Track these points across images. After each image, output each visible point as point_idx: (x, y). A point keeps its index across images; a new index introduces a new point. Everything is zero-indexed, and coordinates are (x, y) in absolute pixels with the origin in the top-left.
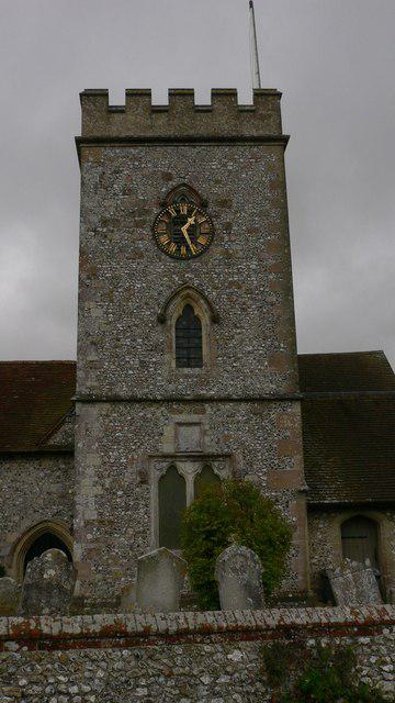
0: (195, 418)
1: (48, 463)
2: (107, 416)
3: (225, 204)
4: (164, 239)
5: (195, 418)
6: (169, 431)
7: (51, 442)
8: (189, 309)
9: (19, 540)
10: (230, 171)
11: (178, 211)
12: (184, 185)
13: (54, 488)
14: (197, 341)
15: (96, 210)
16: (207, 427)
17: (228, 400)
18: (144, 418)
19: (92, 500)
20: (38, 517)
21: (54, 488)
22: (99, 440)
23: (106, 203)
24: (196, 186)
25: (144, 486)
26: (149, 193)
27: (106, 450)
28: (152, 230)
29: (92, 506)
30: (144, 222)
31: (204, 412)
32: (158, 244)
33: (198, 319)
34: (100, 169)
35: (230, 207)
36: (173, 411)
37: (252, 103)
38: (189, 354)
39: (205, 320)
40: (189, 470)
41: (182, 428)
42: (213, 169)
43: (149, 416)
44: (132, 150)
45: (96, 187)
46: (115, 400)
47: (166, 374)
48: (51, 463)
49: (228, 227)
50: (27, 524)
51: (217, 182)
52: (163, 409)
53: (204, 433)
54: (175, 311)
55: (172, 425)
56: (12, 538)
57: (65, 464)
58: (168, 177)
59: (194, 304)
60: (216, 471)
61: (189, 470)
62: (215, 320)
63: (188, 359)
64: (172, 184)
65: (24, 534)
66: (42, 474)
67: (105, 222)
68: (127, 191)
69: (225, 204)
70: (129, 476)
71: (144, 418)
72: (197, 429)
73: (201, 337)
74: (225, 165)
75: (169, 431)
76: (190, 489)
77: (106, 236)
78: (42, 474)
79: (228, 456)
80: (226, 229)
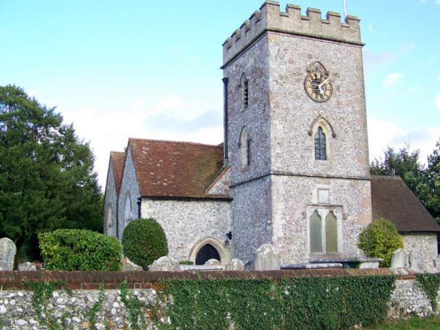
1: (208, 204)
4: (310, 90)
6: (315, 192)
7: (210, 192)
8: (320, 128)
9: (194, 247)
10: (338, 58)
11: (316, 76)
12: (319, 62)
13: (212, 219)
16: (331, 191)
17: (341, 178)
18: (303, 185)
19: (281, 227)
20: (203, 234)
21: (212, 219)
22: (283, 196)
25: (304, 220)
26: (302, 64)
27: (286, 200)
28: (304, 84)
29: (281, 230)
30: (300, 79)
31: (330, 183)
34: (278, 47)
35: (339, 77)
36: (316, 182)
38: (321, 153)
39: (328, 136)
40: (324, 212)
41: (321, 192)
42: (331, 54)
46: (291, 175)
47: (313, 165)
49: (338, 88)
50: (197, 238)
51: (333, 63)
53: (330, 194)
54: (315, 130)
56: (190, 246)
58: (310, 57)
59: (323, 127)
61: (324, 212)
62: (334, 136)
64: (313, 60)
65: (197, 244)
66: (206, 211)
67: (281, 77)
69: (336, 75)
70: (298, 215)
71: (303, 185)
72: (327, 192)
73: (325, 145)
74: (336, 55)
75: (315, 192)
78: (206, 211)
79: (341, 206)
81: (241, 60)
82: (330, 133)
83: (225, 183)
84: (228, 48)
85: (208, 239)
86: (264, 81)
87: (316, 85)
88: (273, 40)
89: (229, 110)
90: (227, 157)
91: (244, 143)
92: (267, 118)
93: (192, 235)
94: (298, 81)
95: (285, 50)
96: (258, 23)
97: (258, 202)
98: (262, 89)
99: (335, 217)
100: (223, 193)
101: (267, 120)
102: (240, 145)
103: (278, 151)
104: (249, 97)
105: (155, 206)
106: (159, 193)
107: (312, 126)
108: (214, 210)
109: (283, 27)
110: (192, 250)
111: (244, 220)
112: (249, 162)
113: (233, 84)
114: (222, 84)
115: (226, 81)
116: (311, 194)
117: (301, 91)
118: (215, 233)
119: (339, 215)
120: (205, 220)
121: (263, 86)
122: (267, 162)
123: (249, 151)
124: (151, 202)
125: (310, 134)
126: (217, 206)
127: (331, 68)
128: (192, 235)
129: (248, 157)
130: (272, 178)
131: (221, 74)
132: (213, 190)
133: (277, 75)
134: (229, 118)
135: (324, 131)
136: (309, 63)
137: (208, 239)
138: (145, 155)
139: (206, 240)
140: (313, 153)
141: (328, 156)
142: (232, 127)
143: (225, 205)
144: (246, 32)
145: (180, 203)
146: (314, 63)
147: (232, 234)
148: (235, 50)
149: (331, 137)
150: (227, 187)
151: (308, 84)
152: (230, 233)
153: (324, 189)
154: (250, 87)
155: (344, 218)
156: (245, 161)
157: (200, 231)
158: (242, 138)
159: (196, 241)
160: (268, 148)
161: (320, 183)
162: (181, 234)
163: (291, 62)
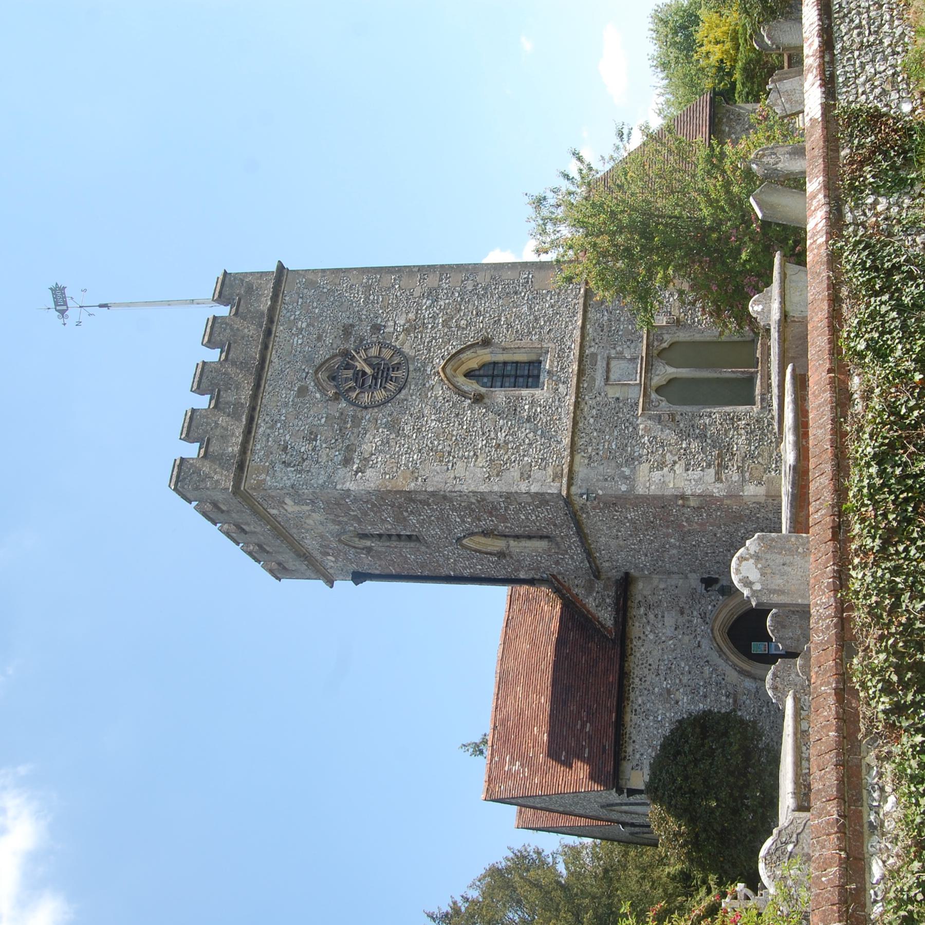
0: (601, 365)
1: (635, 629)
2: (590, 458)
3: (347, 331)
4: (380, 395)
5: (601, 365)
6: (613, 392)
7: (610, 623)
8: (469, 375)
9: (734, 666)
10: (308, 326)
11: (347, 380)
12: (316, 372)
14: (509, 368)
15: (330, 470)
16: (613, 352)
18: (596, 418)
20: (705, 643)
21: (670, 620)
22: (619, 466)
23: (323, 459)
24: (317, 362)
25: (678, 418)
28: (366, 408)
29: (696, 474)
31: (594, 355)
32: (384, 403)
33: (483, 366)
35: (352, 326)
37: (229, 307)
39: (485, 356)
40: (665, 372)
41: (613, 377)
43: (594, 412)
44: (261, 430)
45: (300, 472)
48: (637, 624)
49: (376, 328)
50: (714, 657)
51: (319, 338)
52: (587, 398)
53: (620, 356)
54: (471, 386)
55: (608, 388)
56: (732, 676)
57: (639, 607)
58: (303, 391)
59: (464, 368)
60: (665, 345)
61: (665, 372)
62: (486, 342)
63: (529, 376)
65: (727, 659)
66: (651, 637)
68: (312, 437)
69: (347, 331)
71: (596, 418)
72: (613, 363)
73: (505, 363)
74: (302, 329)
75: (613, 392)
76: (684, 372)
77: (365, 459)
78: (651, 637)
80: (380, 330)
81: (311, 544)
82: (481, 351)
83: (590, 589)
84: (285, 568)
85: (717, 633)
86: (355, 500)
87: (369, 381)
88: (263, 476)
89: (426, 573)
91: (497, 545)
92: (441, 498)
93: (707, 670)
95: (285, 449)
96: (224, 508)
97: (632, 521)
98: (374, 505)
99: (672, 345)
100: (612, 593)
101: (445, 497)
103: (515, 473)
104: (393, 532)
105: (638, 756)
106: (608, 744)
107: (463, 394)
108: (651, 616)
110: (742, 672)
111: (675, 551)
112: (542, 537)
113: (367, 563)
114: (368, 584)
115: (358, 577)
116: (618, 399)
117: (382, 416)
118: (703, 616)
120: (671, 638)
121: (367, 502)
122: (541, 499)
123: (517, 537)
124: (627, 766)
125: (478, 399)
126: (642, 610)
127: (331, 342)
128: (707, 670)
129: (530, 537)
130: (579, 491)
131: (344, 586)
132: (606, 616)
134: (444, 572)
135: (474, 364)
136: (318, 395)
137: (717, 633)
138: (522, 765)
139: (719, 639)
140: (525, 392)
141: (533, 357)
142: (465, 568)
143: (641, 589)
144: (245, 532)
145: (632, 696)
146: (318, 384)
147: (705, 576)
148: (288, 558)
149: (488, 350)
150: (599, 585)
151: (365, 398)
152: (703, 580)
153: (608, 370)
154: (369, 529)
156: (542, 545)
157: (698, 652)
158: (489, 549)
159: (720, 662)
160: (509, 497)
161: (593, 379)
162: (705, 697)
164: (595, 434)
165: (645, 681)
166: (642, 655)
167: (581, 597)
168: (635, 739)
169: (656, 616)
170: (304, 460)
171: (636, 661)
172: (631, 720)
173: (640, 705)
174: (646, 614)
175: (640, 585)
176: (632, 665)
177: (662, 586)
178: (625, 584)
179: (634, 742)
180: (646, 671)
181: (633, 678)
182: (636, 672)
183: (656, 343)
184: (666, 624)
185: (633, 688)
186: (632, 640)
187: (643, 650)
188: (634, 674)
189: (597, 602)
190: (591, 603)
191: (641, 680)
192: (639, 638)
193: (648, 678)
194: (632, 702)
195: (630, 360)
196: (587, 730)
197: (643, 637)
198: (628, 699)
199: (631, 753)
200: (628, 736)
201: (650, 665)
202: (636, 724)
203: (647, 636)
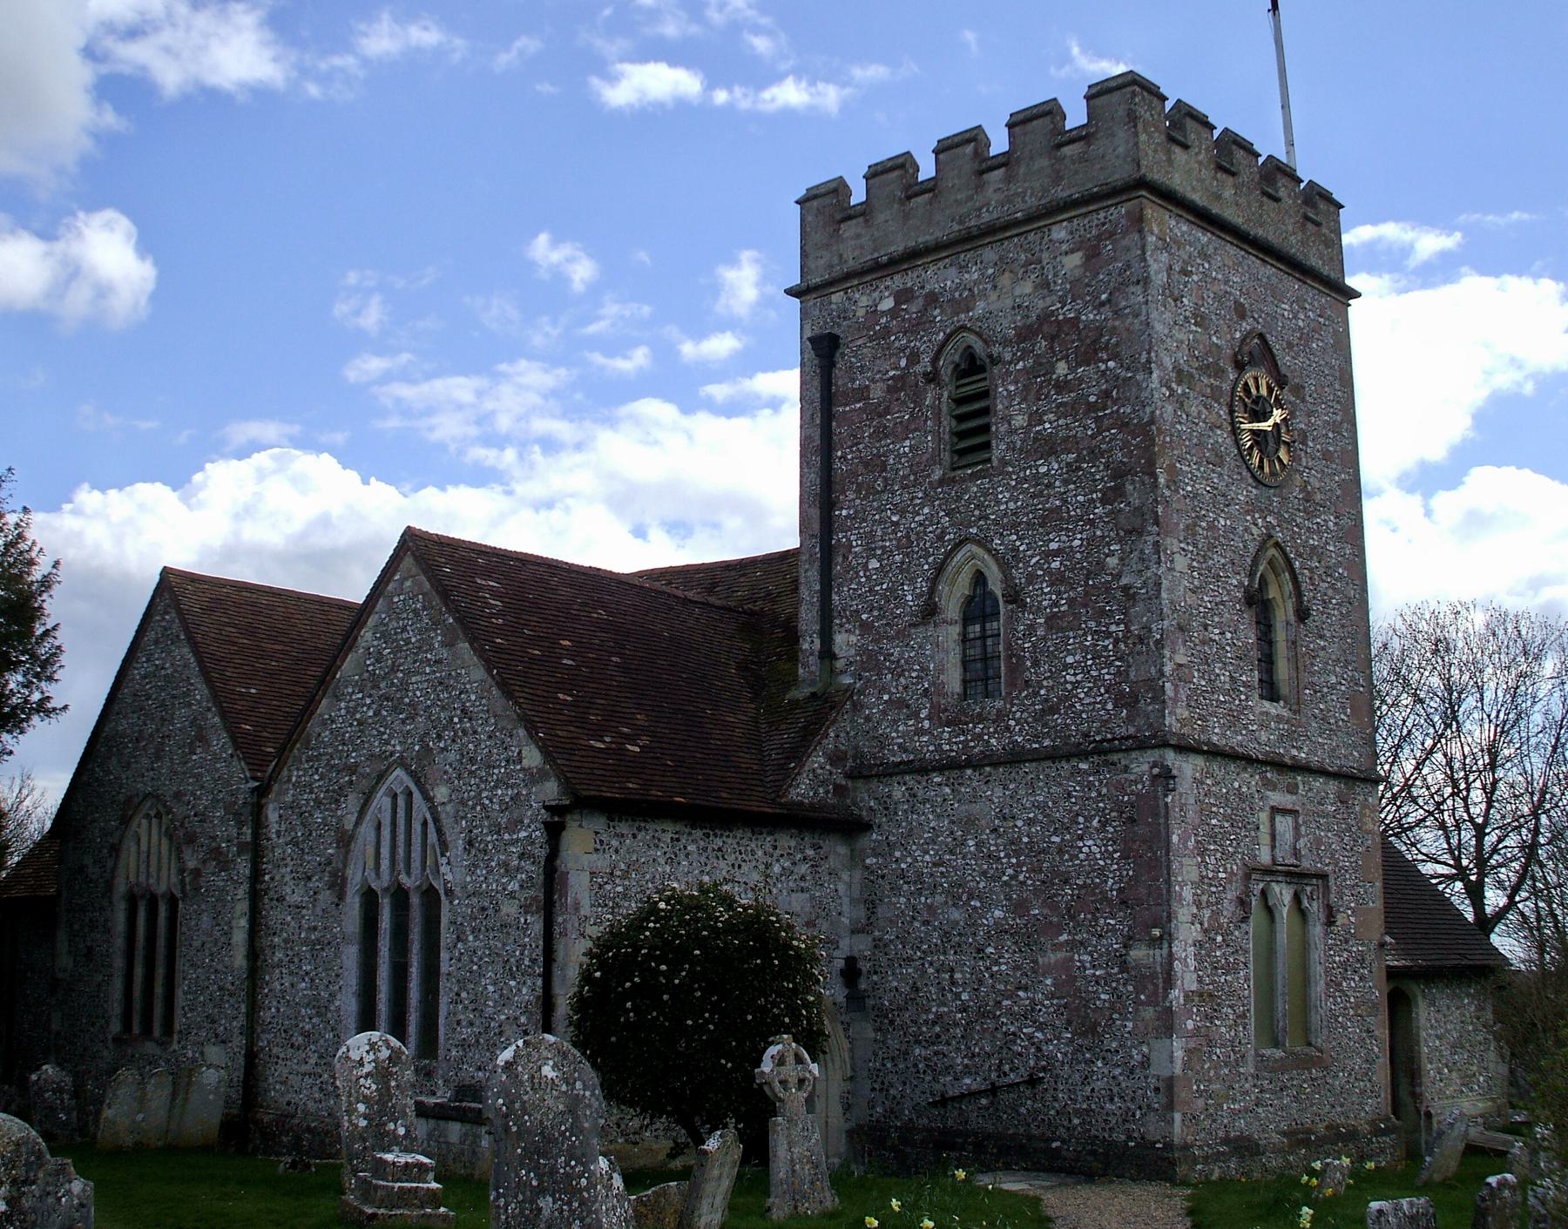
48: (793, 843)
70: (1229, 909)
79: (1323, 877)
90: (827, 654)
94: (1215, 394)
102: (930, 611)
105: (615, 843)
108: (804, 869)
109: (1177, 181)
119: (1315, 908)
124: (599, 823)
126: (810, 852)
132: (802, 790)
133: (1168, 362)
145: (698, 833)
155: (1330, 921)
163: (1201, 320)
164: (1224, 791)
165: (718, 858)
166: (753, 853)
167: (825, 741)
168: (639, 837)
169: (803, 878)
170: (1175, 301)
171: (744, 842)
172: (664, 831)
173: (685, 848)
174: (805, 859)
175: (842, 850)
176: (739, 834)
177: (841, 887)
178: (850, 827)
179: (634, 836)
180: (731, 859)
181: (722, 835)
182: (729, 841)
183: (1309, 889)
184: (793, 895)
185: (708, 836)
186: (770, 833)
187: (760, 853)
188: (728, 836)
189: (819, 771)
190: (817, 760)
191: (720, 849)
192: (775, 848)
193: (722, 864)
194: (690, 834)
195: (1295, 848)
196: (629, 747)
197: (778, 852)
198: (693, 827)
199: (618, 830)
200: (643, 825)
201: (740, 867)
202: (659, 840)
203: (778, 861)
